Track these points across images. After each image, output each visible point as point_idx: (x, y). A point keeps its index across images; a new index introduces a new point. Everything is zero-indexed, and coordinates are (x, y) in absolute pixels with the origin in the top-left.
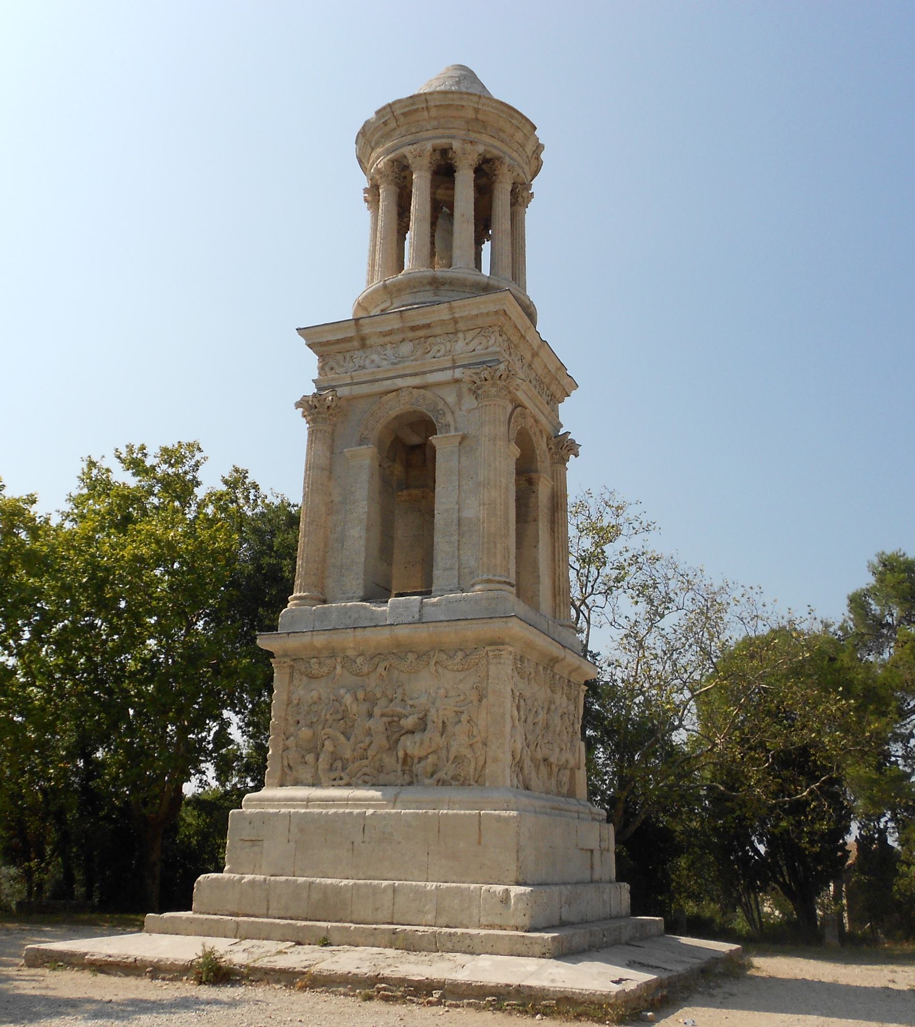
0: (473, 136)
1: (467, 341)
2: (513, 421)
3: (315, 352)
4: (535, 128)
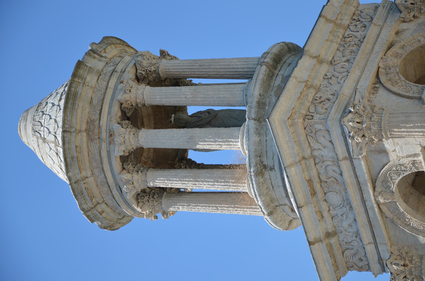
0: (104, 135)
1: (321, 147)
2: (395, 89)
3: (344, 274)
4: (79, 61)
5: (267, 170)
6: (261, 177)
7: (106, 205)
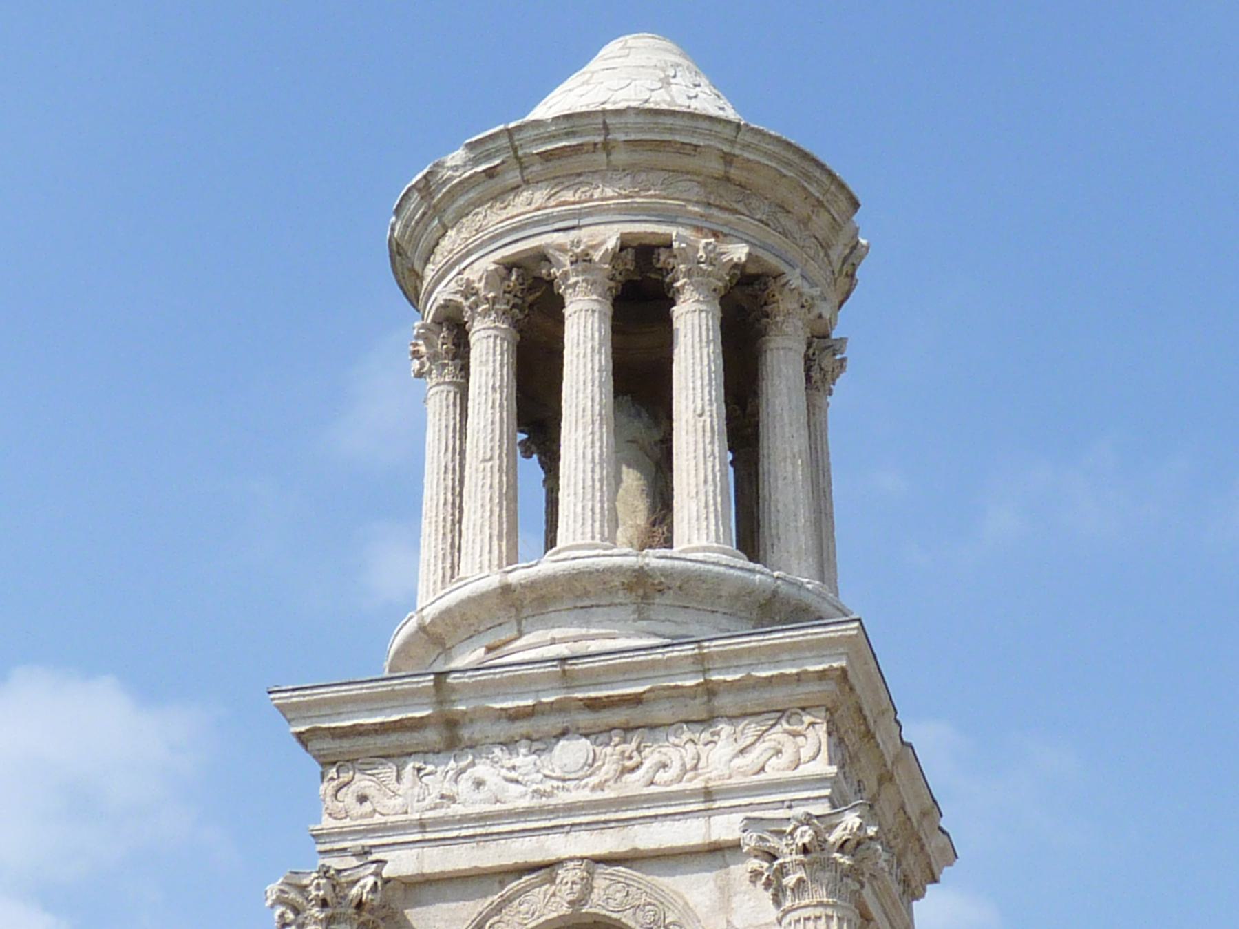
5: (639, 600)
6: (626, 581)
7: (515, 185)
